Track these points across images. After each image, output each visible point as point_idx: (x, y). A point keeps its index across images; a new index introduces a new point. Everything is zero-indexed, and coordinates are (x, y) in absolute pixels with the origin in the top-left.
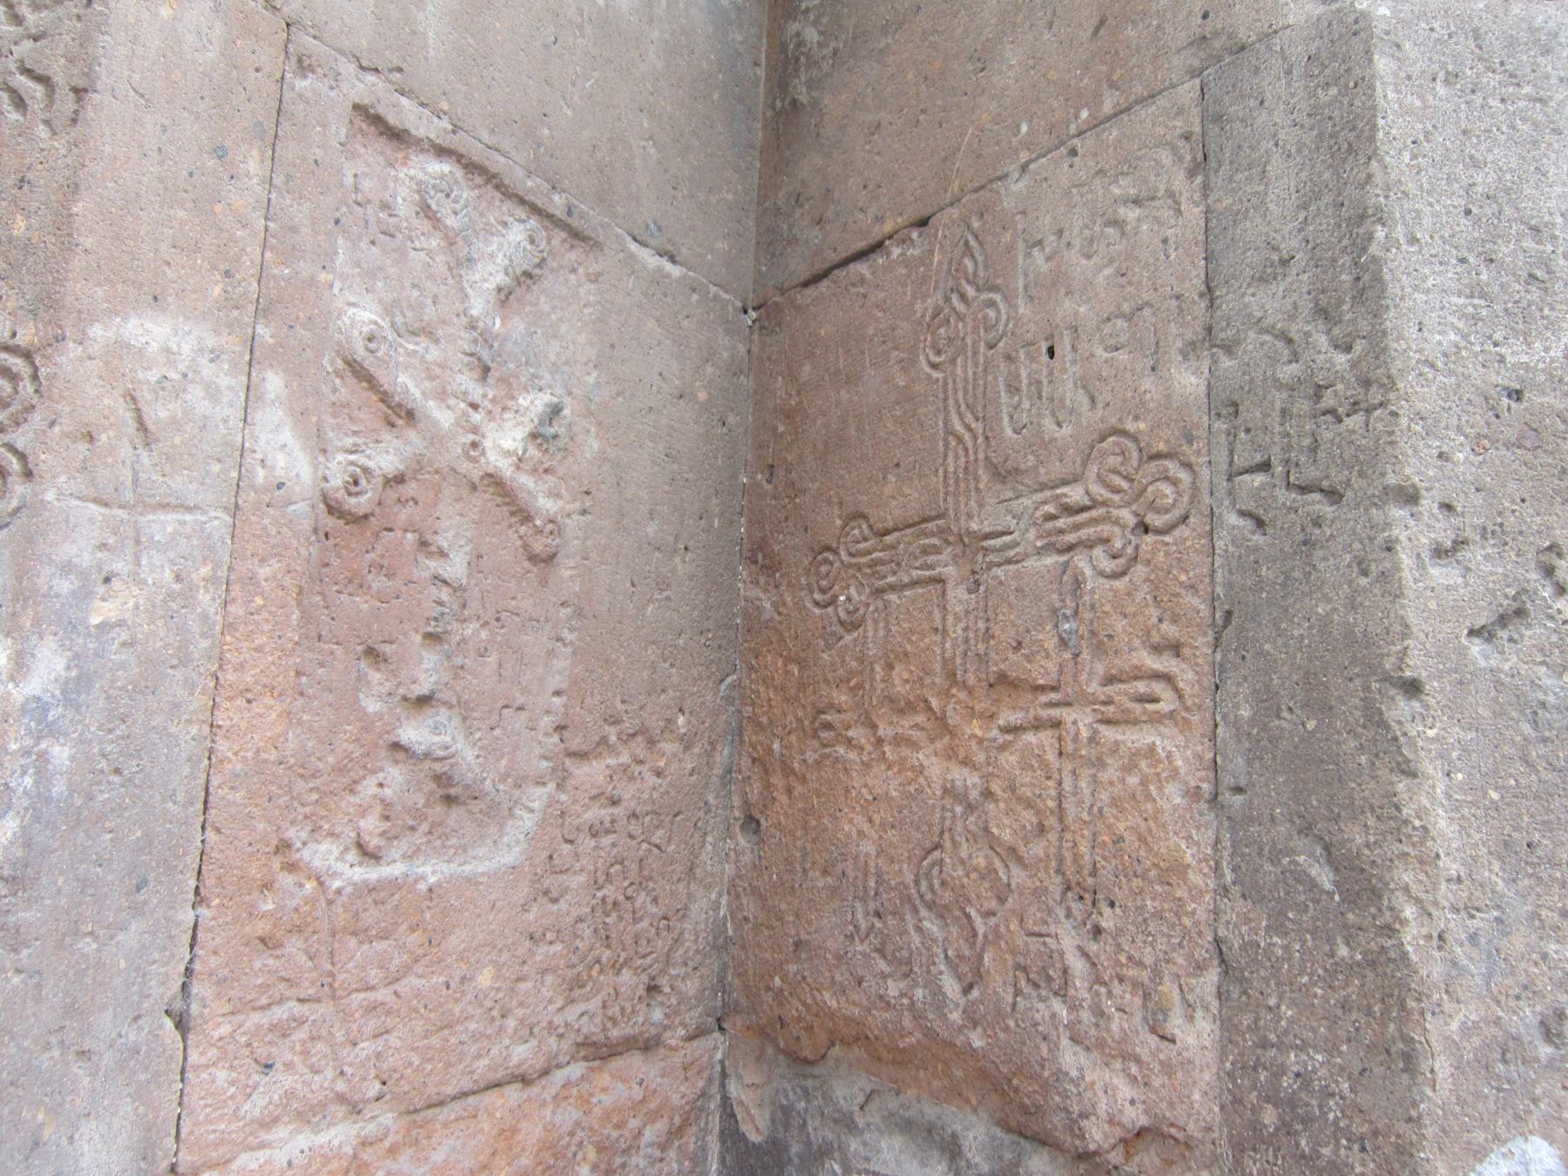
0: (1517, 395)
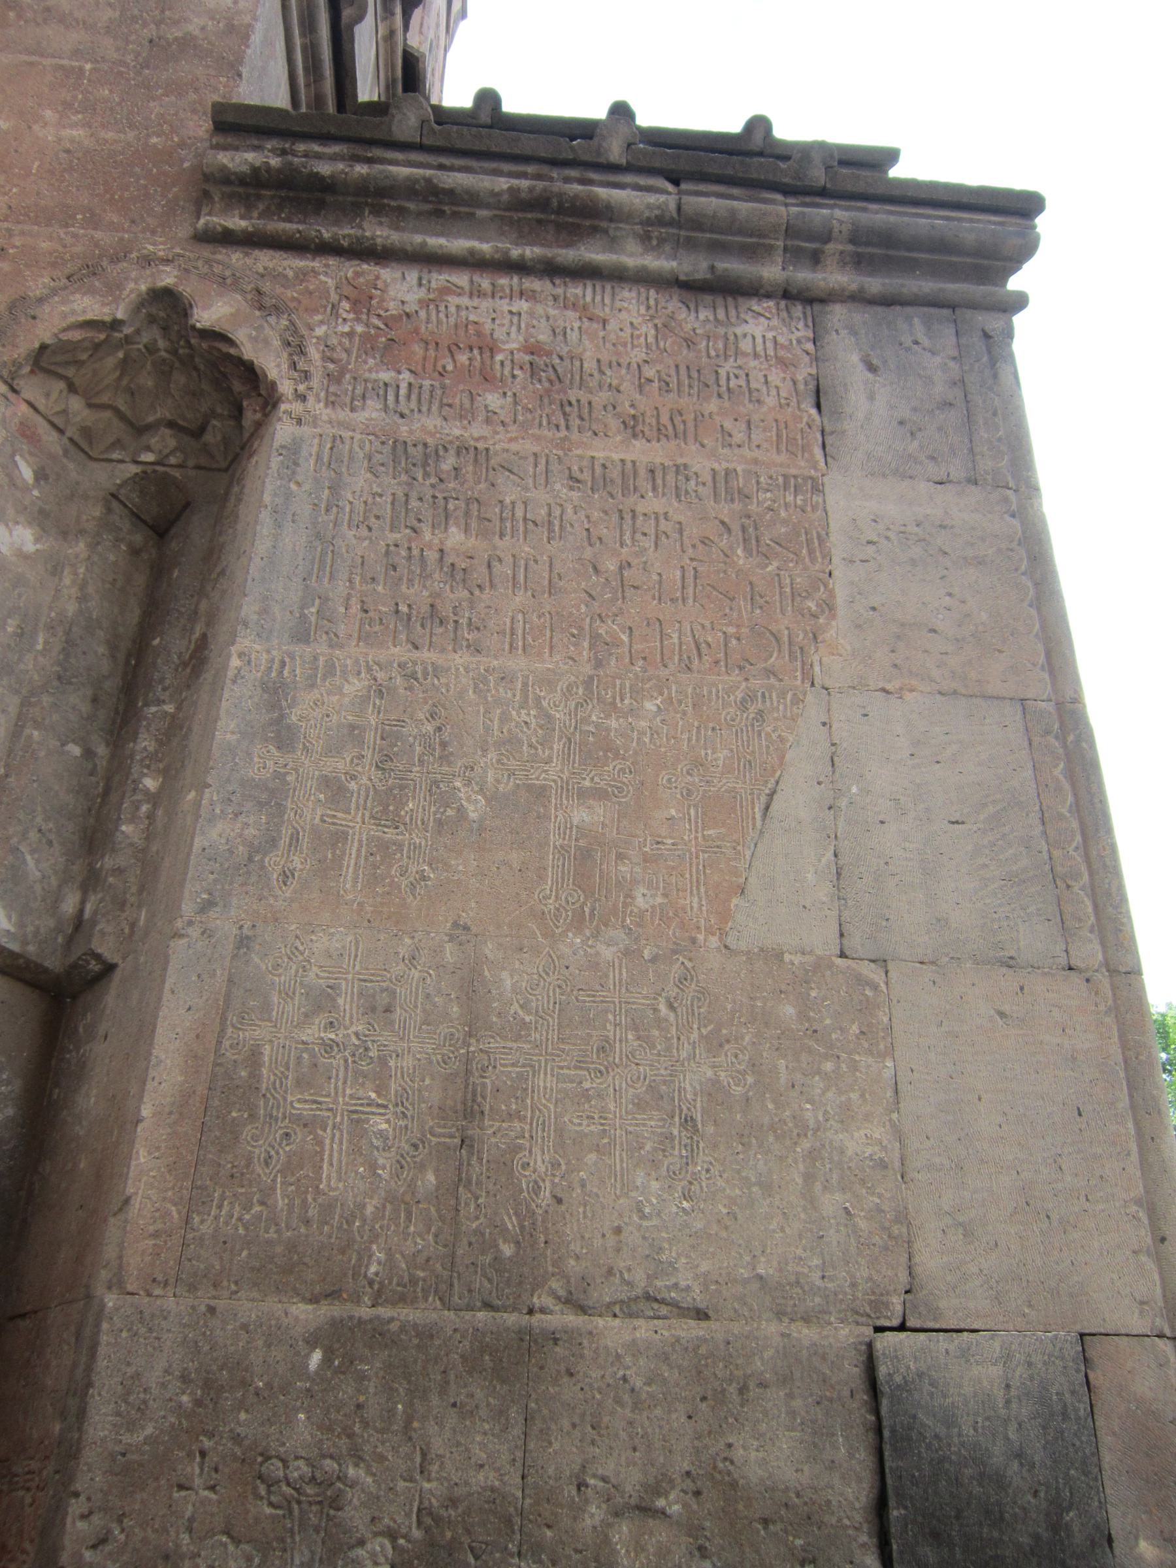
0: (124, 1455)
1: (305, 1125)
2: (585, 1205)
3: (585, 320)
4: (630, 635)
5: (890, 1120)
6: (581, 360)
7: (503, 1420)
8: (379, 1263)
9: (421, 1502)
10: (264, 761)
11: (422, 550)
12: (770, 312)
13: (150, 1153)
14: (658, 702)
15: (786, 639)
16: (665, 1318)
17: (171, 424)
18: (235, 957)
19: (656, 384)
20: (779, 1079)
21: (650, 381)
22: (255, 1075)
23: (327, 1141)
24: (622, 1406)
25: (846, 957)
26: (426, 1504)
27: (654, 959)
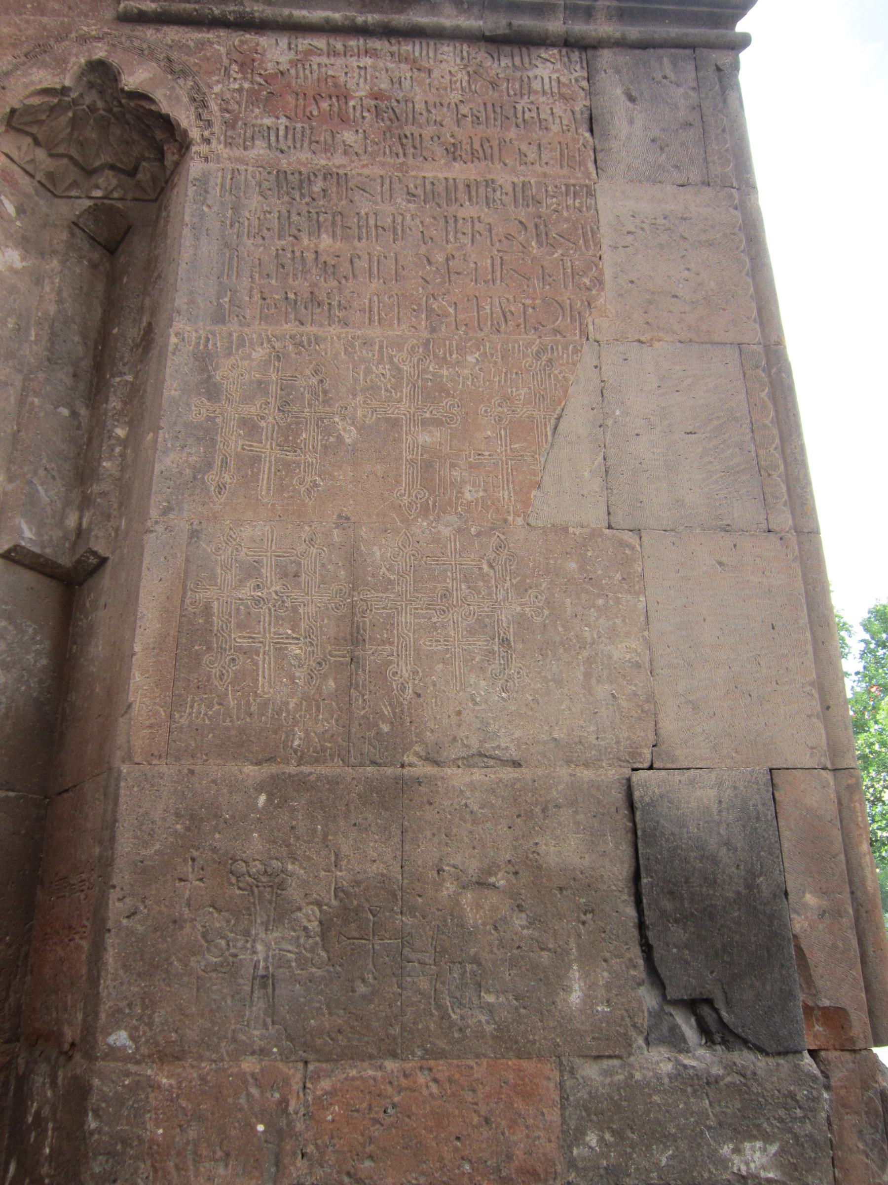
0: (142, 862)
1: (245, 653)
2: (436, 698)
3: (415, 70)
4: (456, 308)
5: (643, 636)
6: (413, 103)
7: (387, 833)
8: (300, 739)
9: (336, 884)
10: (198, 410)
11: (302, 252)
12: (555, 58)
13: (142, 675)
14: (477, 355)
15: (568, 306)
16: (492, 767)
17: (112, 167)
18: (189, 544)
19: (469, 119)
20: (566, 611)
21: (465, 116)
22: (208, 622)
23: (261, 663)
24: (465, 822)
25: (612, 528)
26: (340, 885)
27: (479, 534)
